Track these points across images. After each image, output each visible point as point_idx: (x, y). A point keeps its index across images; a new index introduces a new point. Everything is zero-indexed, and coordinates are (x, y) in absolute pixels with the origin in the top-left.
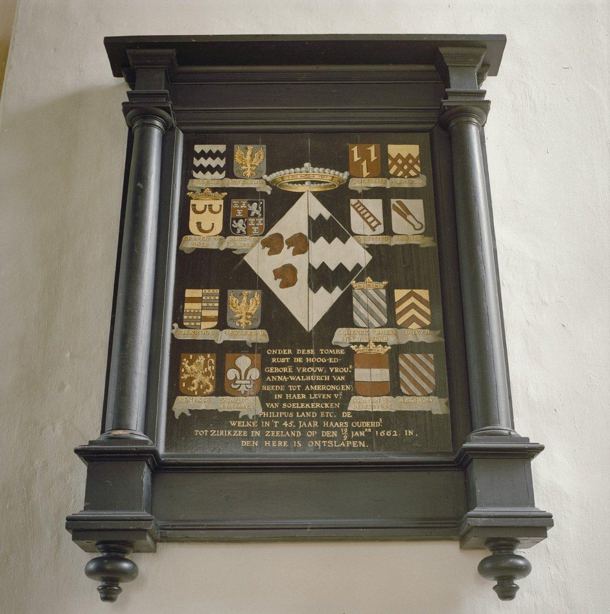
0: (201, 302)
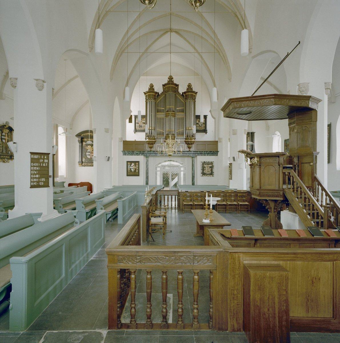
0: (197, 125)
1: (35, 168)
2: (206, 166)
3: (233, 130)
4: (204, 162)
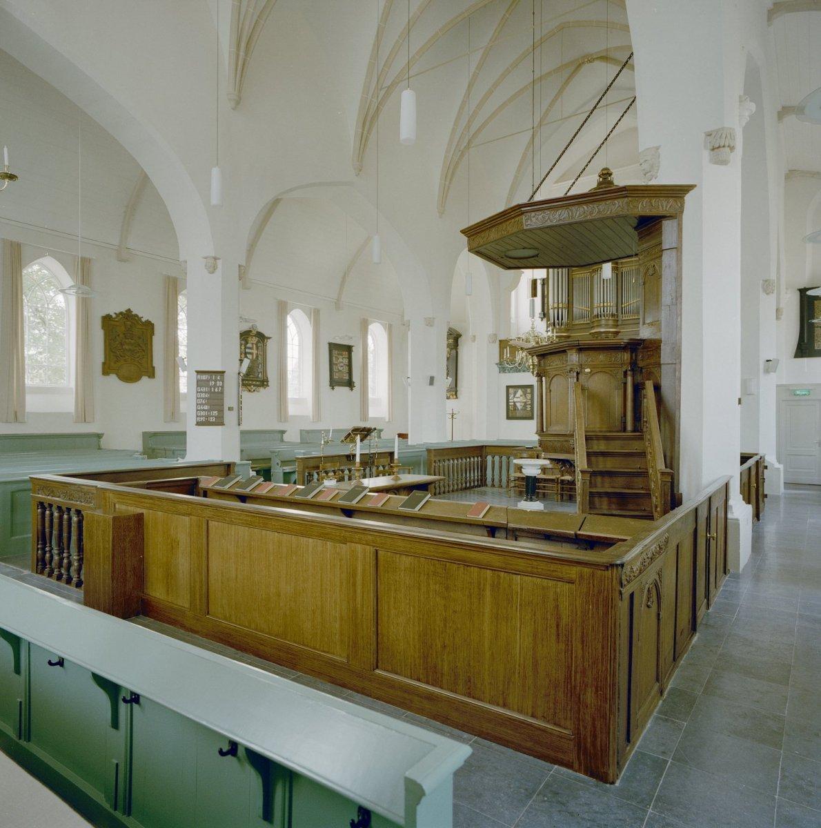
1: (203, 395)
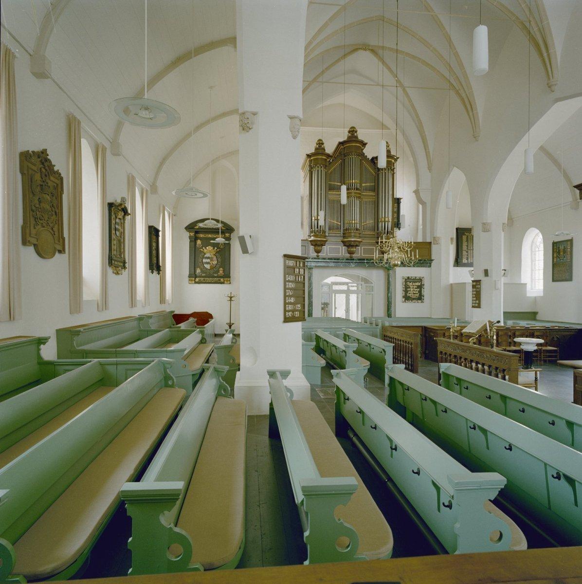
2: (411, 284)
3: (484, 224)
4: (408, 277)
